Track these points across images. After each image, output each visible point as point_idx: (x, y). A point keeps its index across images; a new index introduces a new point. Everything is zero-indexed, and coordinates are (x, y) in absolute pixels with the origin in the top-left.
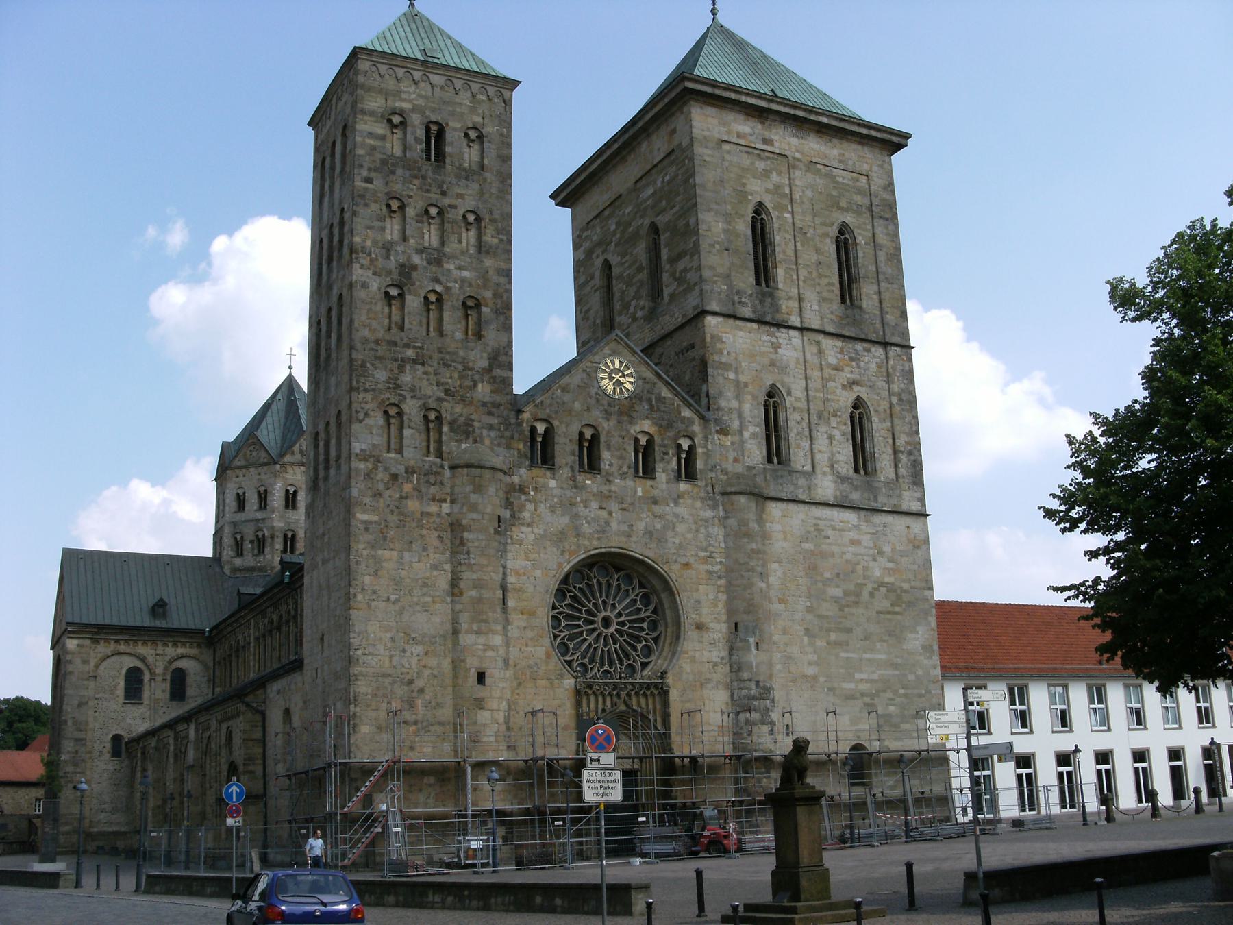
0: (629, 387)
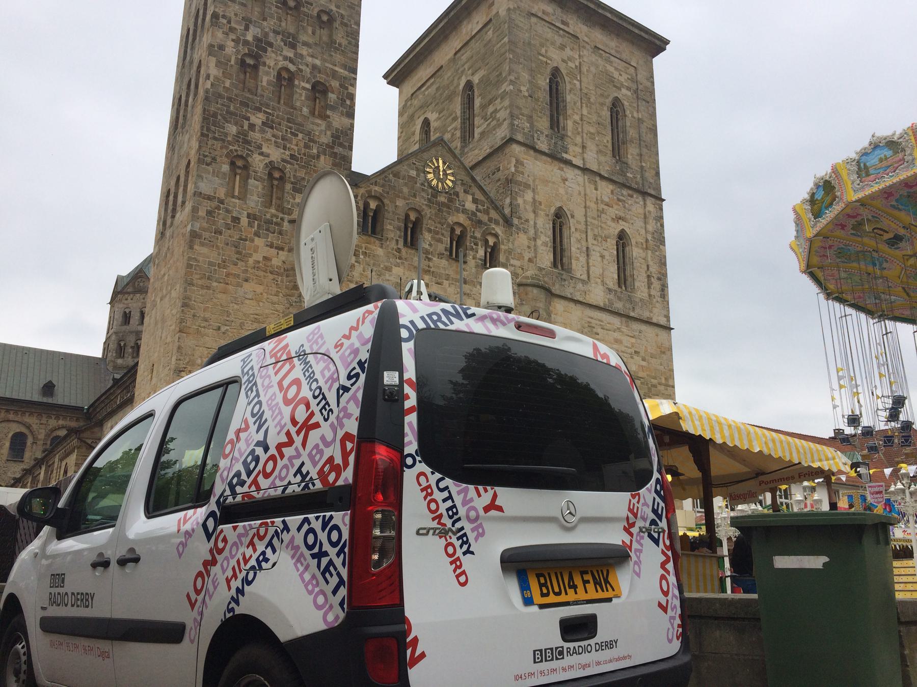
0: (450, 184)
